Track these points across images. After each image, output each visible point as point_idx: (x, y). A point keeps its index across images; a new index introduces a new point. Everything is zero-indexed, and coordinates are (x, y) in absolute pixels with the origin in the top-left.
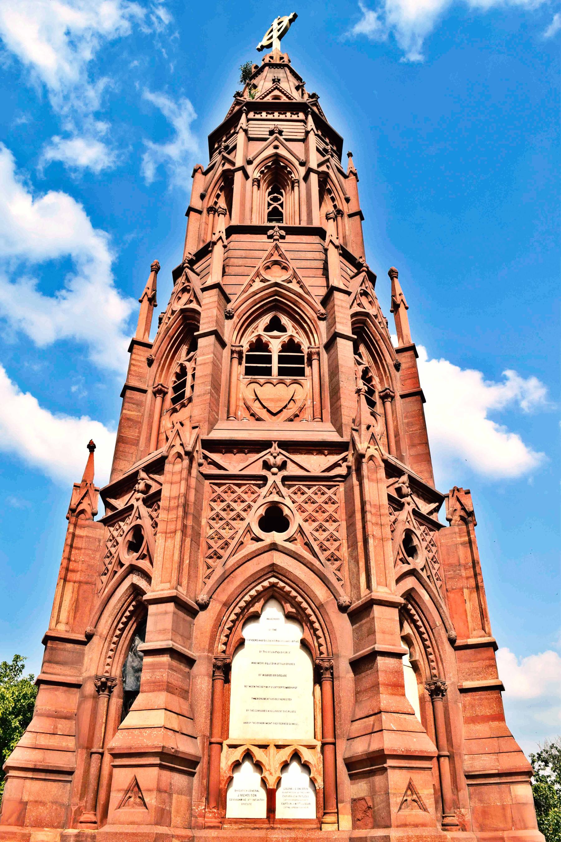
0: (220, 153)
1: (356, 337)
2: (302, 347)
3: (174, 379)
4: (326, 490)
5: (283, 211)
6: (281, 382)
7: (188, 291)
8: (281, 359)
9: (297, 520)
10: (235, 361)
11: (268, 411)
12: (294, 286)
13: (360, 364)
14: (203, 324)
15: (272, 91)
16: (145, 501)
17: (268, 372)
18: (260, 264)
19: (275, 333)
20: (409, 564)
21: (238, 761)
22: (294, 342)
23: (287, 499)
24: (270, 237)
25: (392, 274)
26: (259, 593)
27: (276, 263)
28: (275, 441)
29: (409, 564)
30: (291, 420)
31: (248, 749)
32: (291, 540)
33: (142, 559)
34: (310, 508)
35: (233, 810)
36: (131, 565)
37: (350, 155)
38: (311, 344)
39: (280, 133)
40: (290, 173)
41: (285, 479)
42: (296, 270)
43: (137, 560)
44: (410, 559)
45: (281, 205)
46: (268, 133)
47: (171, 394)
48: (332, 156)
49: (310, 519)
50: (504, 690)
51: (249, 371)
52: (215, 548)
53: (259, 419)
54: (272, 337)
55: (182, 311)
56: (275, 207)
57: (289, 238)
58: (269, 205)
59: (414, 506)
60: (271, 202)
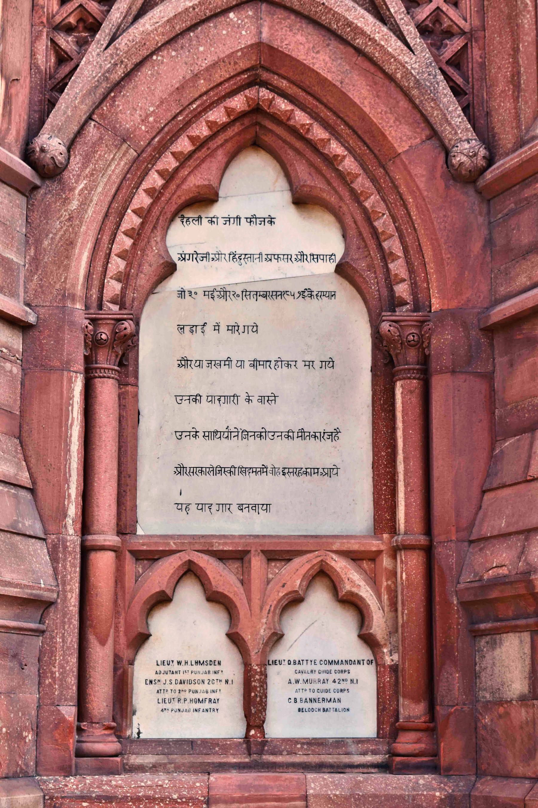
21: (163, 592)
26: (217, 130)
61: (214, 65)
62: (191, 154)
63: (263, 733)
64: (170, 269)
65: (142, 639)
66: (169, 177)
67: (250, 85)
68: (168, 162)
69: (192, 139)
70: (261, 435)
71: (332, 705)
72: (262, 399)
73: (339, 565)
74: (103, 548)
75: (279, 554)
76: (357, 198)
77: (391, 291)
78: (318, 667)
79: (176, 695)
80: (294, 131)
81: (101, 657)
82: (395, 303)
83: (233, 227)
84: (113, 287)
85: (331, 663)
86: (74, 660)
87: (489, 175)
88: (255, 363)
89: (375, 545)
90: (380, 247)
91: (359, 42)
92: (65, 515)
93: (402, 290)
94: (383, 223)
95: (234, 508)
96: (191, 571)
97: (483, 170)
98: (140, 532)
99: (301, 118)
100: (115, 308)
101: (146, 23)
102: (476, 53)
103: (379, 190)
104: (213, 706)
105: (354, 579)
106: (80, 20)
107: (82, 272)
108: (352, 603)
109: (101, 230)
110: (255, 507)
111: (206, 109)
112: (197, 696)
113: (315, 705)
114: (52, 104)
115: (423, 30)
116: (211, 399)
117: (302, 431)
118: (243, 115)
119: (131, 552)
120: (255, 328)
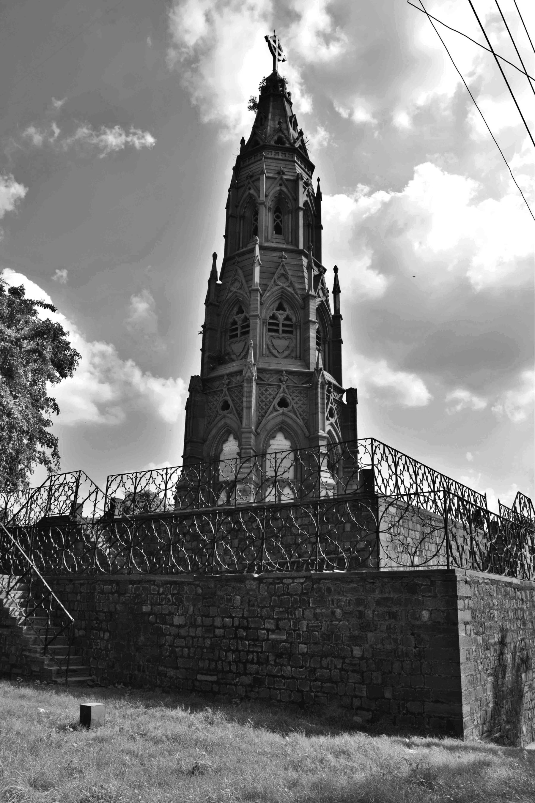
2: (293, 320)
3: (230, 325)
6: (284, 338)
8: (284, 325)
9: (292, 403)
14: (253, 311)
16: (228, 389)
19: (281, 312)
25: (336, 269)
27: (283, 275)
32: (290, 411)
34: (297, 399)
37: (319, 180)
39: (284, 173)
41: (287, 386)
42: (292, 279)
44: (330, 418)
45: (281, 221)
49: (296, 403)
53: (276, 357)
55: (235, 292)
56: (278, 224)
58: (275, 221)
68: (271, 433)
84: (264, 448)
101: (271, 416)
115: (302, 419)
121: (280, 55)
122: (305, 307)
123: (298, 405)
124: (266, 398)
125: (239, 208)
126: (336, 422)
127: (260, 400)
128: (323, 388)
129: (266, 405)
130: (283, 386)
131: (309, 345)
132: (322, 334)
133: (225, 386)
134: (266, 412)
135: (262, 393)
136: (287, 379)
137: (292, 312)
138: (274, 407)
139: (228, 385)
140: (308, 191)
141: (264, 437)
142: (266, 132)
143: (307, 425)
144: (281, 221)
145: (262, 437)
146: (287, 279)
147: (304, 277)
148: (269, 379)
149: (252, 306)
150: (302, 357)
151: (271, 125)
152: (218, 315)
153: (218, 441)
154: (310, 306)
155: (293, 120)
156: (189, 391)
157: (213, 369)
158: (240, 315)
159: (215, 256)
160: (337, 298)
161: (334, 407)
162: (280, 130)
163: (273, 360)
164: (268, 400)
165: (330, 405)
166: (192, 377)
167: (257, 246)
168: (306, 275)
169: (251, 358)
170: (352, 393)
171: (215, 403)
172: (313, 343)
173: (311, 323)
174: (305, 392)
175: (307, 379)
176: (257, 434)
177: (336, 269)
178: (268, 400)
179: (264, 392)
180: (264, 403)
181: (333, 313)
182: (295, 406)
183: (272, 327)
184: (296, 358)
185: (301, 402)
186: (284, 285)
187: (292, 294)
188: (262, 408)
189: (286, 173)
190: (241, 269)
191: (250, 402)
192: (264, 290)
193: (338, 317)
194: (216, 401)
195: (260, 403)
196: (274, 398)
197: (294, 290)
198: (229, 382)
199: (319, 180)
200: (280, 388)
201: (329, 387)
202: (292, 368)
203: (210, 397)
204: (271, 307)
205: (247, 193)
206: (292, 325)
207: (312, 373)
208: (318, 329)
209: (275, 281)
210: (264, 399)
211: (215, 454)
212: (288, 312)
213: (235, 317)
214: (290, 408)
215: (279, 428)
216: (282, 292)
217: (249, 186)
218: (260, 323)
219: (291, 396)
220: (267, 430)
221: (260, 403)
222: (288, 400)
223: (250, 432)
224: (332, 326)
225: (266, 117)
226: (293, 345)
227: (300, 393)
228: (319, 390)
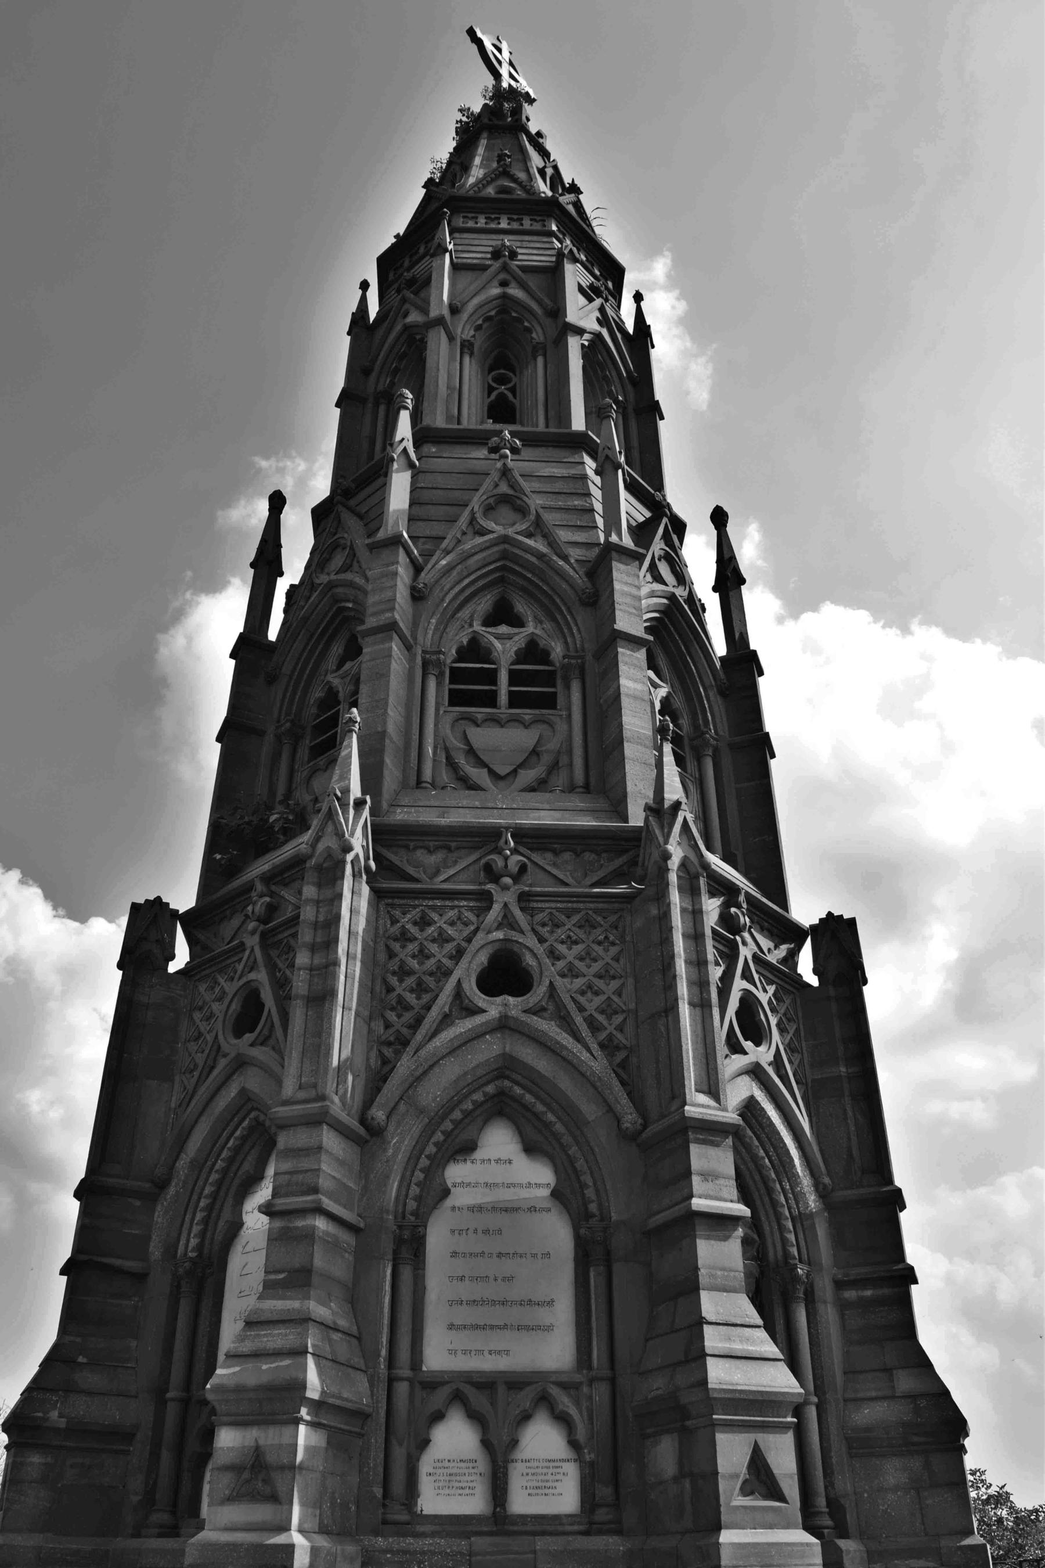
0: (398, 291)
1: (651, 638)
3: (314, 710)
4: (599, 919)
5: (516, 402)
7: (344, 549)
8: (515, 678)
9: (547, 974)
10: (432, 684)
11: (492, 773)
12: (537, 544)
13: (655, 686)
15: (497, 177)
16: (264, 936)
17: (490, 699)
18: (476, 502)
19: (503, 629)
20: (746, 1053)
21: (440, 1411)
22: (538, 644)
23: (530, 935)
24: (494, 450)
26: (477, 1105)
27: (504, 500)
28: (507, 828)
29: (746, 1053)
30: (532, 789)
31: (457, 1389)
32: (537, 1011)
33: (262, 1044)
35: (433, 1501)
36: (239, 1055)
37: (638, 297)
38: (568, 650)
39: (513, 255)
40: (529, 330)
41: (524, 898)
42: (541, 511)
43: (252, 1045)
44: (748, 1045)
45: (513, 390)
46: (489, 256)
47: (307, 742)
48: (607, 300)
49: (571, 972)
50: (916, 1282)
51: (456, 699)
52: (398, 1026)
54: (498, 637)
55: (331, 586)
56: (501, 396)
57: (527, 453)
58: (491, 390)
59: (756, 949)
60: (494, 385)
61: (478, 1066)
62: (462, 1119)
63: (505, 1509)
64: (446, 1193)
65: (425, 1443)
66: (447, 1134)
67: (497, 1078)
68: (448, 1125)
69: (462, 1111)
70: (503, 1303)
71: (551, 1491)
72: (504, 1279)
73: (554, 1391)
74: (402, 1379)
75: (516, 1382)
76: (564, 1148)
77: (586, 1209)
78: (541, 1464)
79: (447, 1484)
80: (526, 1107)
81: (399, 1453)
82: (589, 1216)
83: (486, 1165)
84: (412, 1205)
85: (550, 1461)
86: (382, 1456)
87: (644, 1135)
88: (500, 1255)
89: (578, 1378)
90: (579, 1181)
91: (564, 1053)
92: (379, 1356)
93: (593, 1207)
94: (581, 1164)
95: (486, 1353)
96: (458, 1398)
97: (641, 1132)
98: (424, 1369)
99: (529, 1098)
100: (413, 1218)
101: (437, 1042)
102: (634, 1060)
103: (577, 1143)
104: (471, 1491)
105: (565, 1402)
106: (397, 1038)
107: (393, 1195)
108: (562, 1419)
109: (405, 1169)
110: (499, 1352)
111: (470, 1093)
112: (461, 1485)
113: (539, 1491)
114: (379, 1090)
115: (602, 1046)
116: (472, 1279)
117: (530, 1301)
118: (494, 1096)
119: (421, 1383)
120: (500, 1232)
121: (511, 76)
122: (598, 596)
123: (579, 982)
124: (423, 955)
125: (374, 375)
126: (777, 1062)
127: (394, 965)
128: (691, 890)
129: (420, 988)
130: (504, 897)
131: (620, 725)
132: (684, 721)
133: (251, 926)
134: (419, 1021)
135: (404, 932)
136: (523, 869)
137: (548, 625)
138: (459, 993)
139: (264, 920)
140: (602, 310)
141: (408, 1143)
142: (464, 185)
143: (623, 1070)
144: (513, 390)
145: (400, 1143)
146: (522, 511)
147: (593, 510)
148: (437, 872)
149: (371, 600)
150: (593, 780)
151: (476, 173)
152: (272, 679)
153: (219, 1184)
154: (617, 586)
155: (549, 171)
156: (120, 966)
157: (232, 870)
158: (348, 665)
159: (277, 501)
160: (733, 601)
161: (764, 998)
162: (505, 172)
163: (466, 798)
164: (430, 964)
165: (739, 984)
166: (135, 907)
167: (404, 420)
168: (598, 507)
169: (346, 776)
170: (838, 937)
171: (216, 1007)
172: (637, 721)
173: (620, 642)
174: (613, 918)
175: (619, 862)
176: (367, 1136)
177: (719, 518)
178: (430, 964)
179: (414, 930)
180: (410, 981)
181: (720, 647)
182: (559, 982)
183: (469, 684)
184: (571, 789)
185: (596, 967)
186: (510, 532)
187: (541, 556)
188: (403, 1006)
189: (520, 257)
190: (360, 517)
191: (326, 969)
192: (428, 555)
193: (744, 663)
194: (220, 999)
195: (394, 981)
196: (458, 955)
197: (552, 544)
198: (272, 909)
199: (638, 297)
200: (489, 908)
201: (725, 906)
202: (545, 815)
203: (202, 988)
204: (465, 613)
205: (398, 328)
206: (552, 673)
207: (638, 830)
208: (666, 702)
209: (473, 520)
210: (414, 964)
211: (200, 1248)
212: (531, 628)
213: (330, 678)
214: (538, 994)
215: (489, 1098)
216: (504, 556)
217: (407, 306)
218: (411, 660)
219: (542, 940)
220: (421, 1111)
221: (394, 981)
222: (529, 960)
223: (318, 1120)
224: (722, 693)
225: (466, 168)
226: (553, 745)
227: (587, 924)
228: (675, 897)
